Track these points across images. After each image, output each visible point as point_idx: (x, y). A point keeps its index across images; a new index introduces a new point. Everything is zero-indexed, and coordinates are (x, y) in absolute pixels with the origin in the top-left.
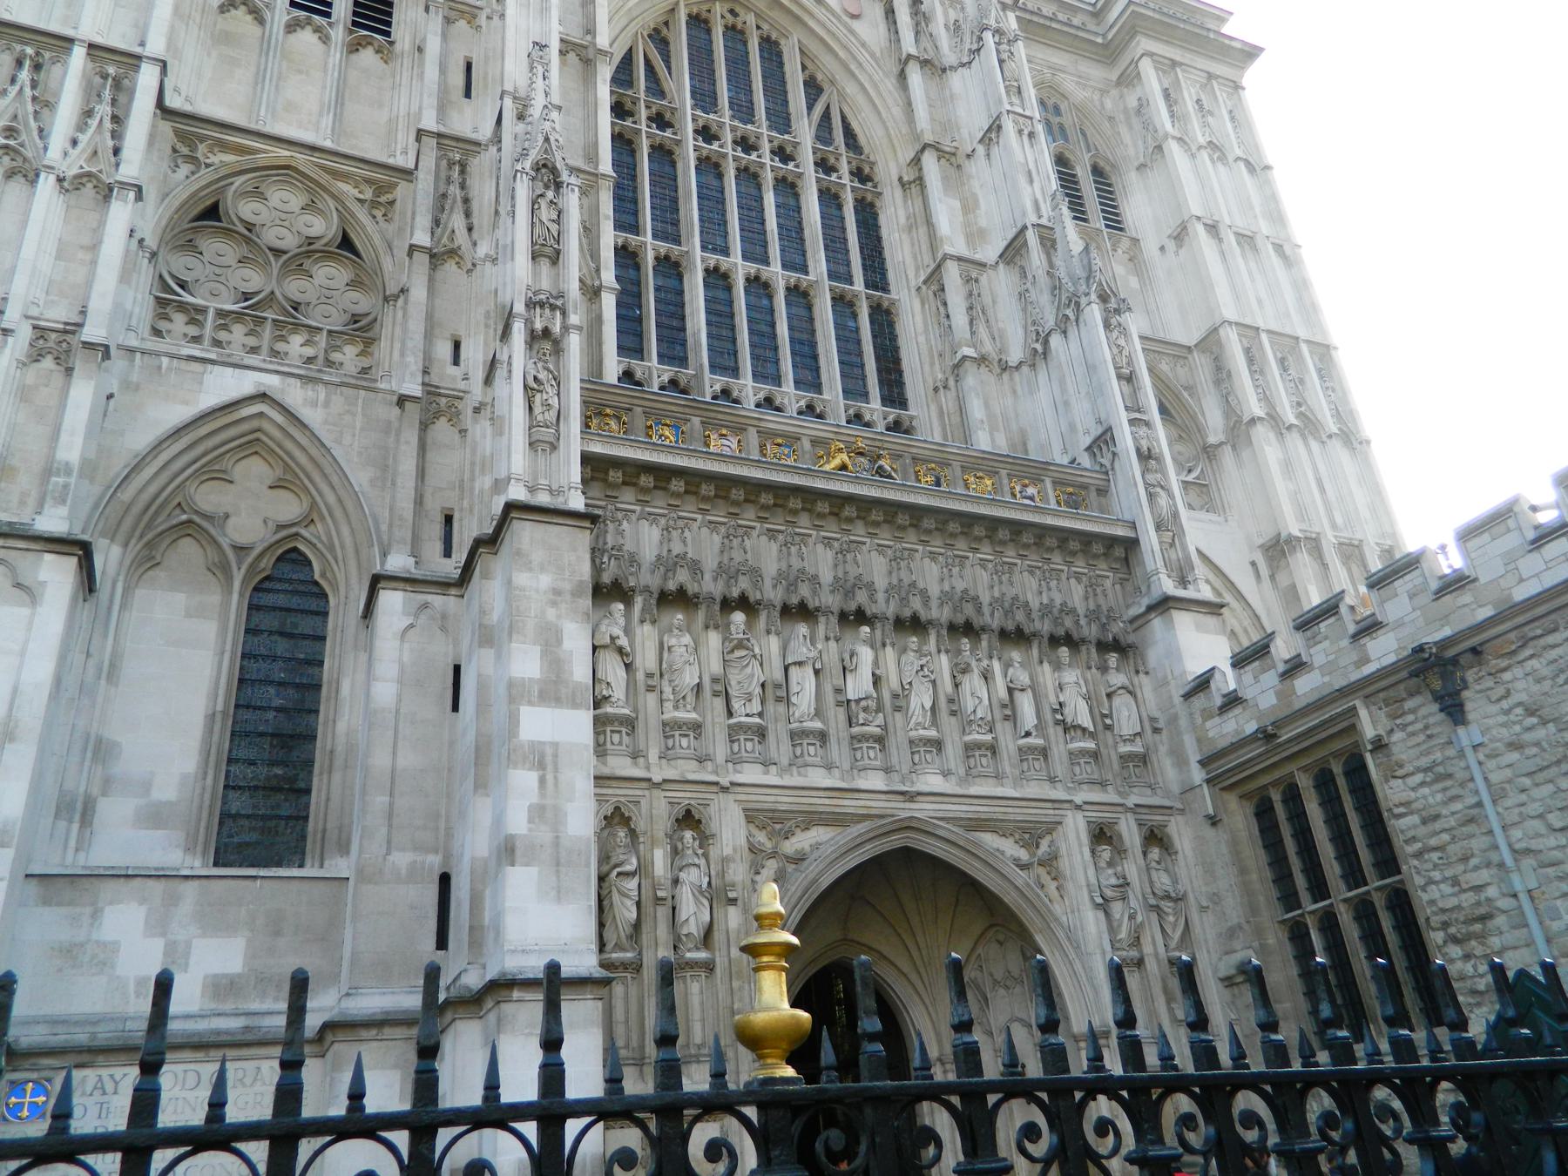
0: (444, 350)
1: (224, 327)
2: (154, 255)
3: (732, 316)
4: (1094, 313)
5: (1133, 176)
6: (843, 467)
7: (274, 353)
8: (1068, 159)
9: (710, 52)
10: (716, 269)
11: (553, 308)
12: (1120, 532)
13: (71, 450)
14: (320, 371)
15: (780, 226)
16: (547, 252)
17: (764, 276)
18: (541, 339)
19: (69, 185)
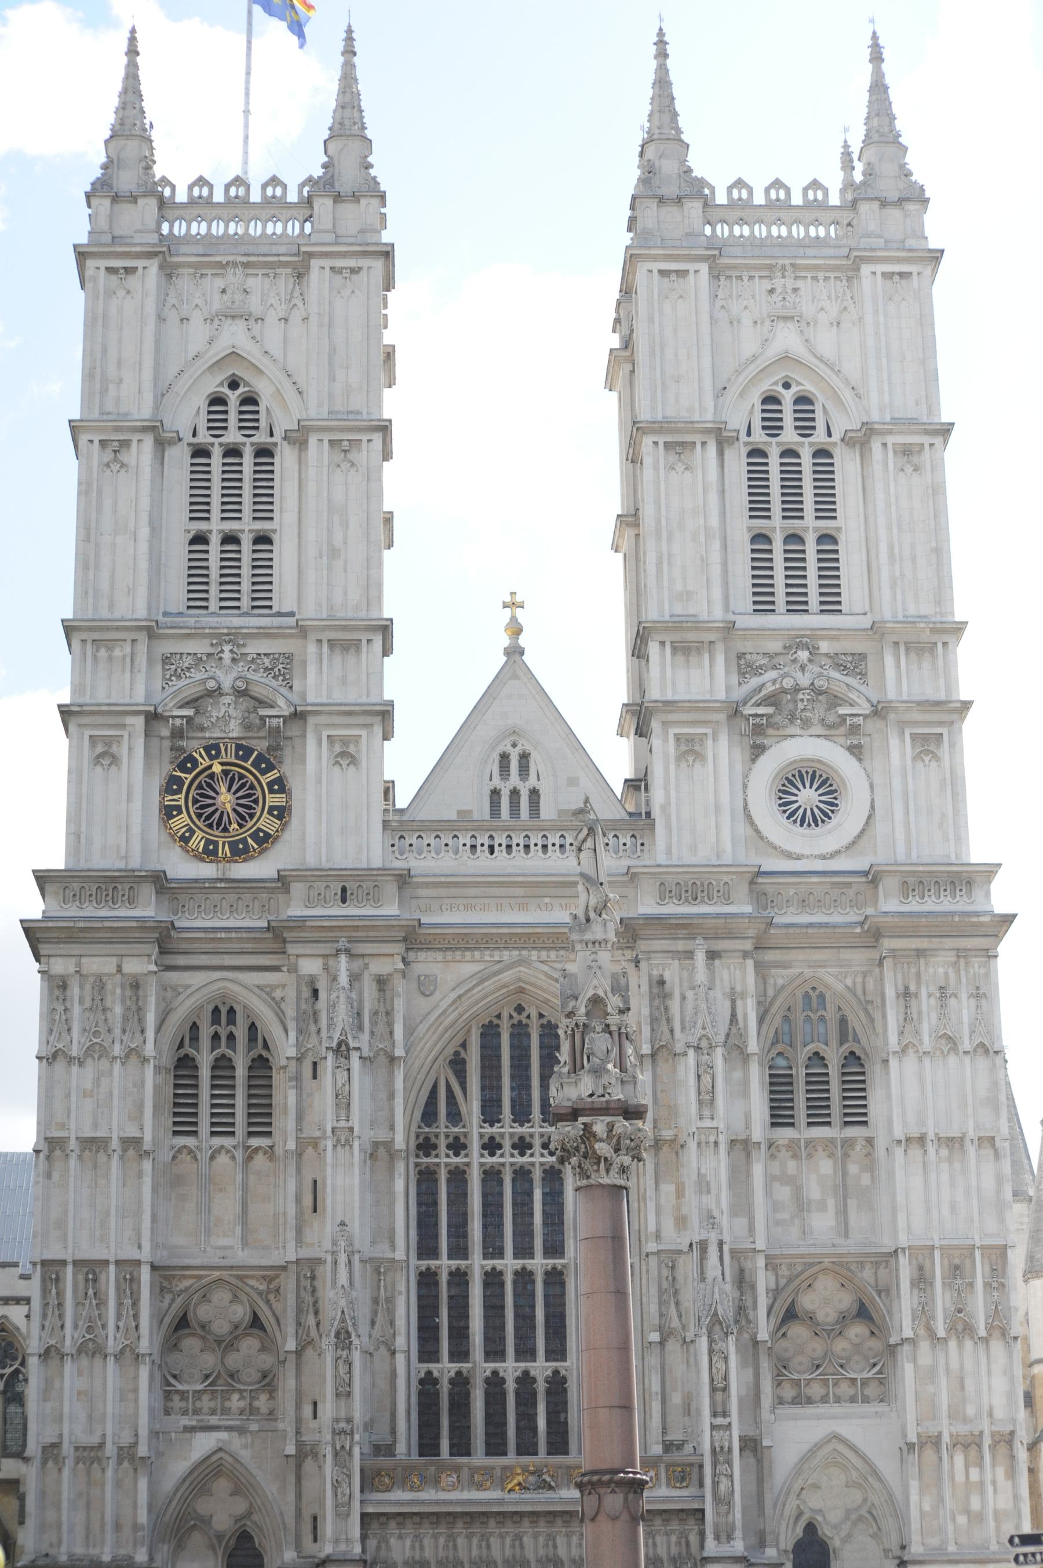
0: (307, 1410)
1: (199, 1399)
2: (160, 1366)
3: (502, 1307)
4: (703, 1343)
5: (878, 1067)
6: (519, 1484)
7: (225, 1411)
8: (823, 1058)
9: (499, 1057)
10: (494, 1269)
11: (345, 1433)
12: (696, 1506)
13: (143, 1517)
14: (248, 1419)
15: (544, 1212)
16: (343, 1393)
17: (529, 1268)
18: (341, 1456)
19: (118, 1357)
